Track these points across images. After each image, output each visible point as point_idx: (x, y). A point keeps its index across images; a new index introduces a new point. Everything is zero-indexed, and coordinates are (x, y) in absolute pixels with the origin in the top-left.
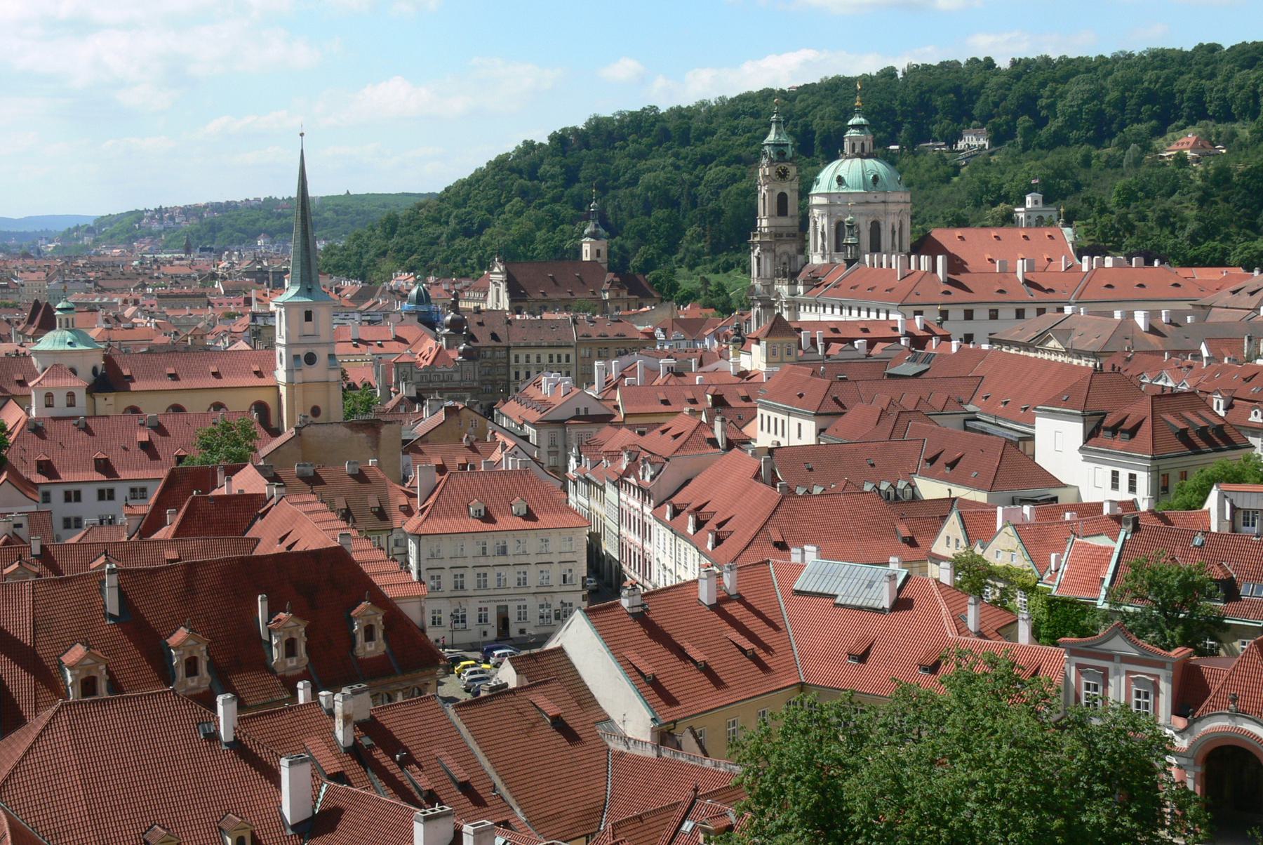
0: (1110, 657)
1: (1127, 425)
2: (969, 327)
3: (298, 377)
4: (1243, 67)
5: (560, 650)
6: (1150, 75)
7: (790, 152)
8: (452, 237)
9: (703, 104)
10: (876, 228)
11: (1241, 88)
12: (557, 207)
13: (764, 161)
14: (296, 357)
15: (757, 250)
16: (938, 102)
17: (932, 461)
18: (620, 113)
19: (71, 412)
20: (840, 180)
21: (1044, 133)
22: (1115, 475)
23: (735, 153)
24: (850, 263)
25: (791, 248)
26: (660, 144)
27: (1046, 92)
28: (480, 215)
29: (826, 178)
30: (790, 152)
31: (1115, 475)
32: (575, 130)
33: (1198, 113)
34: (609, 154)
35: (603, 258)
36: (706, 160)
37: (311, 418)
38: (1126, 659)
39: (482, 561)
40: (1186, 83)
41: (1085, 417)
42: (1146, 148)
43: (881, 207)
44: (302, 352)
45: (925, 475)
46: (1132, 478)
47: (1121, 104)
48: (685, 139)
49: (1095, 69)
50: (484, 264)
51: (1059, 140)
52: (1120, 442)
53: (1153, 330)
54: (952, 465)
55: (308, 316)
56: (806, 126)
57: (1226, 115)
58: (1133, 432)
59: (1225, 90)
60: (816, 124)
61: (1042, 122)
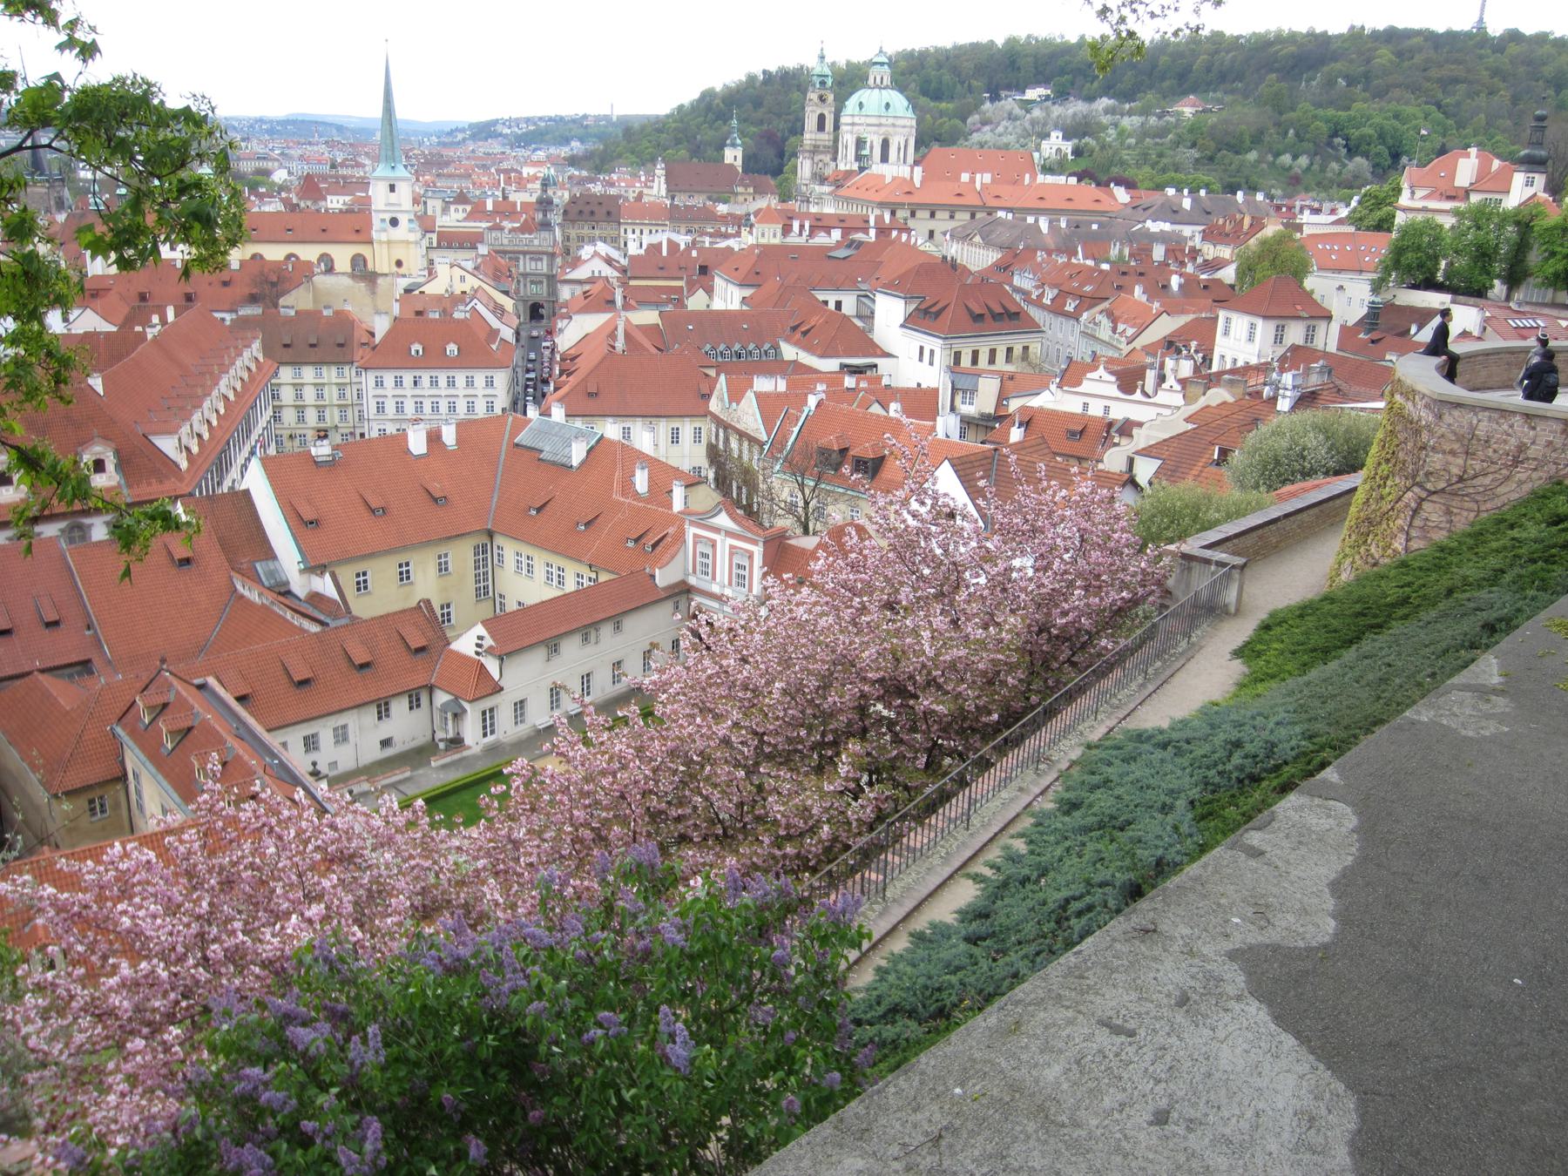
0: (717, 530)
1: (933, 310)
2: (932, 225)
5: (247, 493)
7: (829, 82)
10: (885, 144)
14: (383, 220)
17: (794, 329)
20: (861, 105)
22: (922, 348)
25: (827, 158)
29: (852, 104)
30: (829, 82)
31: (922, 348)
32: (764, 72)
35: (739, 163)
37: (395, 269)
38: (729, 534)
39: (417, 392)
43: (891, 130)
44: (388, 217)
45: (788, 340)
46: (932, 352)
50: (653, 161)
54: (805, 333)
55: (392, 188)
58: (938, 314)
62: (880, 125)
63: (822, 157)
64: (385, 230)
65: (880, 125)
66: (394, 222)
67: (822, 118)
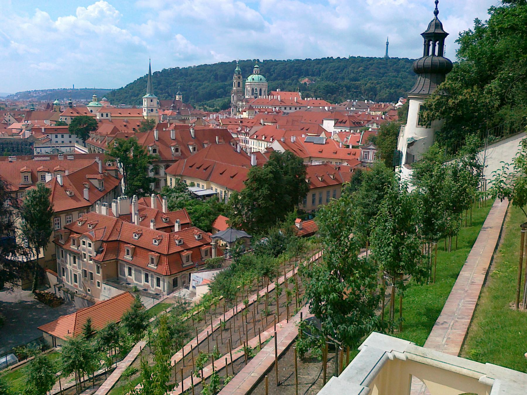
0: (370, 149)
3: (149, 114)
4: (317, 64)
6: (296, 65)
7: (241, 73)
8: (131, 96)
9: (190, 67)
11: (316, 69)
12: (157, 90)
13: (235, 75)
14: (149, 110)
15: (233, 95)
16: (247, 69)
18: (170, 68)
19: (107, 118)
20: (253, 79)
21: (272, 77)
23: (199, 79)
24: (256, 97)
26: (181, 76)
27: (272, 68)
28: (137, 92)
29: (250, 78)
33: (307, 75)
34: (168, 78)
35: (181, 100)
36: (192, 80)
38: (373, 149)
40: (304, 67)
41: (335, 120)
42: (298, 81)
44: (150, 109)
47: (289, 71)
48: (186, 76)
49: (283, 63)
51: (275, 79)
52: (342, 125)
53: (329, 111)
55: (152, 101)
56: (216, 73)
57: (313, 75)
58: (345, 122)
59: (313, 69)
60: (219, 73)
61: (271, 75)
62: (259, 85)
63: (240, 94)
64: (150, 113)
65: (259, 85)
66: (152, 110)
67: (239, 83)
